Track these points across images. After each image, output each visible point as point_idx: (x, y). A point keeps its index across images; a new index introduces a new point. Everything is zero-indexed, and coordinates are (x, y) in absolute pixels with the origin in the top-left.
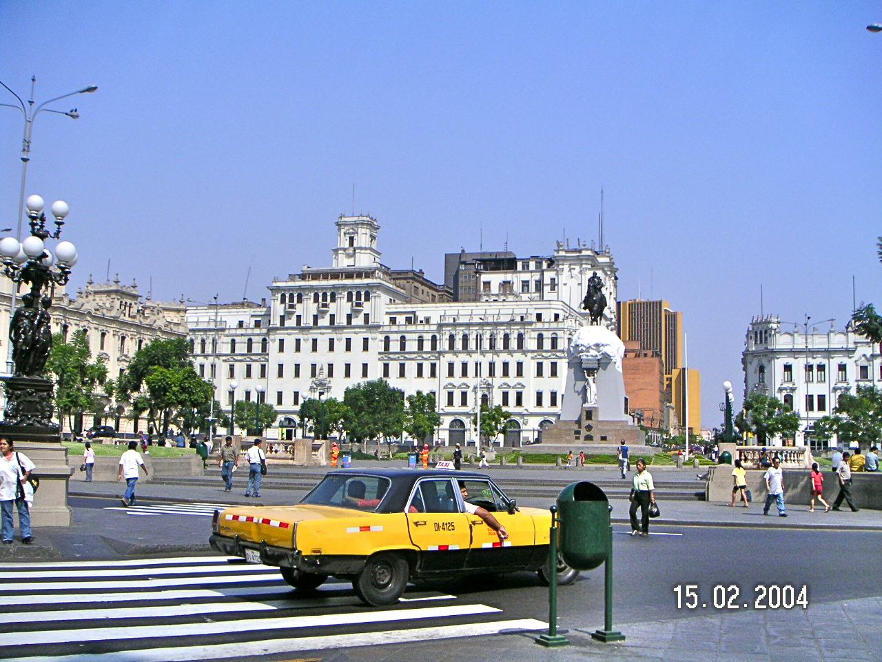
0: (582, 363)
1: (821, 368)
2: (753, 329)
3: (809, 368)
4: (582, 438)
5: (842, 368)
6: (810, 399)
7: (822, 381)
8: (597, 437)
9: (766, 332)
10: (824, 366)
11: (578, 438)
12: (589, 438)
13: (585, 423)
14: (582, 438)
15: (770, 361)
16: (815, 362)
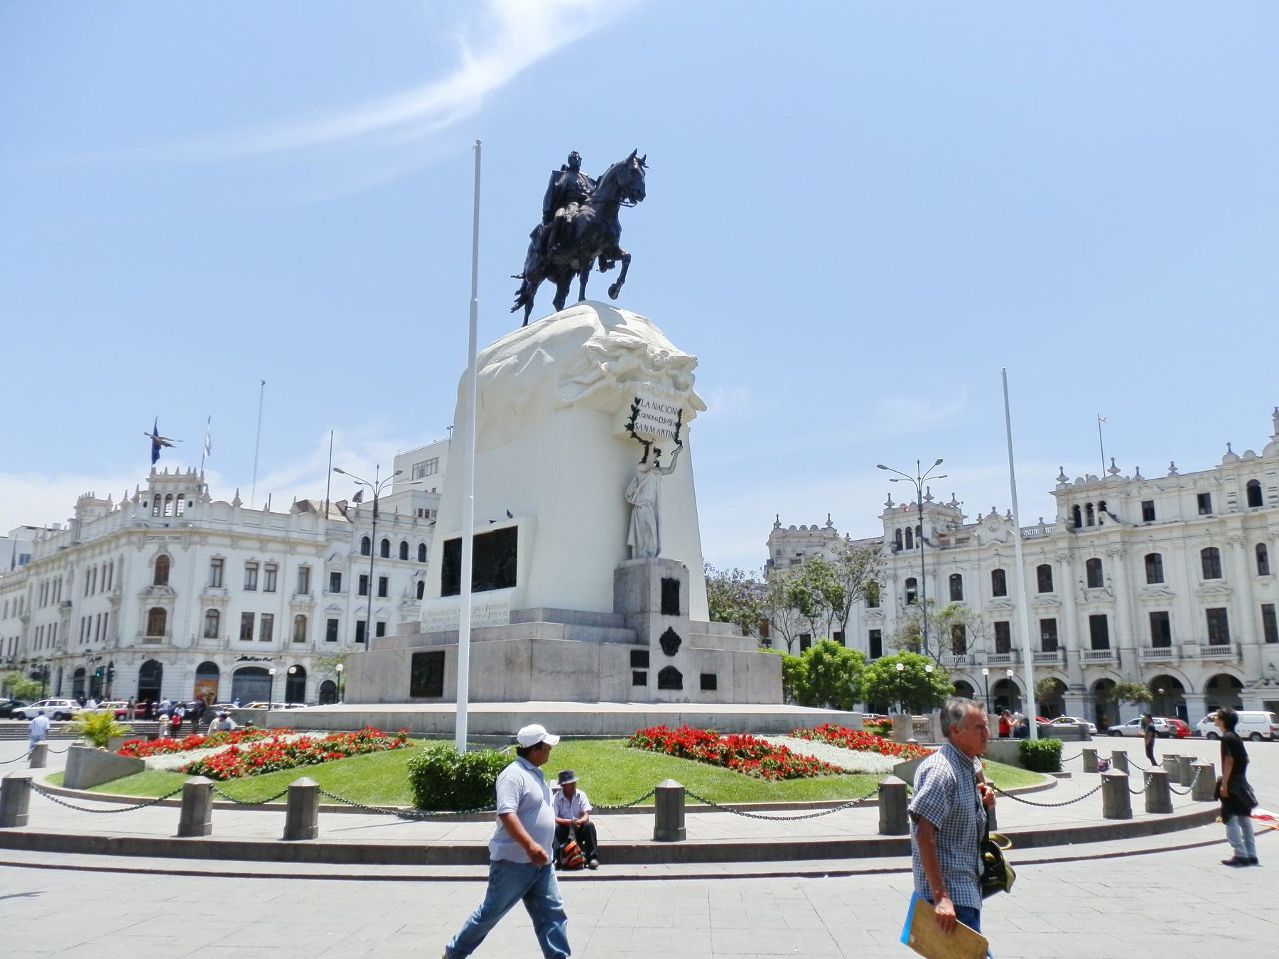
0: (636, 412)
1: (273, 570)
2: (152, 488)
3: (252, 568)
4: (653, 680)
5: (305, 572)
6: (248, 619)
7: (270, 589)
8: (691, 680)
9: (180, 497)
10: (276, 566)
11: (640, 679)
12: (671, 679)
13: (658, 624)
14: (653, 680)
15: (186, 549)
16: (262, 558)
